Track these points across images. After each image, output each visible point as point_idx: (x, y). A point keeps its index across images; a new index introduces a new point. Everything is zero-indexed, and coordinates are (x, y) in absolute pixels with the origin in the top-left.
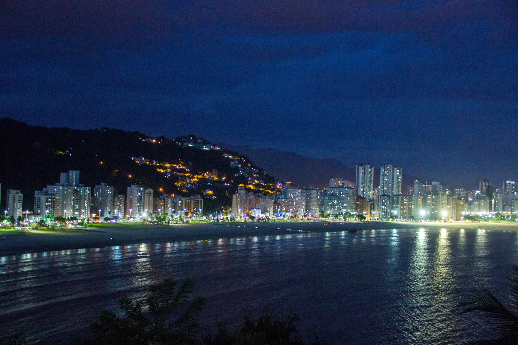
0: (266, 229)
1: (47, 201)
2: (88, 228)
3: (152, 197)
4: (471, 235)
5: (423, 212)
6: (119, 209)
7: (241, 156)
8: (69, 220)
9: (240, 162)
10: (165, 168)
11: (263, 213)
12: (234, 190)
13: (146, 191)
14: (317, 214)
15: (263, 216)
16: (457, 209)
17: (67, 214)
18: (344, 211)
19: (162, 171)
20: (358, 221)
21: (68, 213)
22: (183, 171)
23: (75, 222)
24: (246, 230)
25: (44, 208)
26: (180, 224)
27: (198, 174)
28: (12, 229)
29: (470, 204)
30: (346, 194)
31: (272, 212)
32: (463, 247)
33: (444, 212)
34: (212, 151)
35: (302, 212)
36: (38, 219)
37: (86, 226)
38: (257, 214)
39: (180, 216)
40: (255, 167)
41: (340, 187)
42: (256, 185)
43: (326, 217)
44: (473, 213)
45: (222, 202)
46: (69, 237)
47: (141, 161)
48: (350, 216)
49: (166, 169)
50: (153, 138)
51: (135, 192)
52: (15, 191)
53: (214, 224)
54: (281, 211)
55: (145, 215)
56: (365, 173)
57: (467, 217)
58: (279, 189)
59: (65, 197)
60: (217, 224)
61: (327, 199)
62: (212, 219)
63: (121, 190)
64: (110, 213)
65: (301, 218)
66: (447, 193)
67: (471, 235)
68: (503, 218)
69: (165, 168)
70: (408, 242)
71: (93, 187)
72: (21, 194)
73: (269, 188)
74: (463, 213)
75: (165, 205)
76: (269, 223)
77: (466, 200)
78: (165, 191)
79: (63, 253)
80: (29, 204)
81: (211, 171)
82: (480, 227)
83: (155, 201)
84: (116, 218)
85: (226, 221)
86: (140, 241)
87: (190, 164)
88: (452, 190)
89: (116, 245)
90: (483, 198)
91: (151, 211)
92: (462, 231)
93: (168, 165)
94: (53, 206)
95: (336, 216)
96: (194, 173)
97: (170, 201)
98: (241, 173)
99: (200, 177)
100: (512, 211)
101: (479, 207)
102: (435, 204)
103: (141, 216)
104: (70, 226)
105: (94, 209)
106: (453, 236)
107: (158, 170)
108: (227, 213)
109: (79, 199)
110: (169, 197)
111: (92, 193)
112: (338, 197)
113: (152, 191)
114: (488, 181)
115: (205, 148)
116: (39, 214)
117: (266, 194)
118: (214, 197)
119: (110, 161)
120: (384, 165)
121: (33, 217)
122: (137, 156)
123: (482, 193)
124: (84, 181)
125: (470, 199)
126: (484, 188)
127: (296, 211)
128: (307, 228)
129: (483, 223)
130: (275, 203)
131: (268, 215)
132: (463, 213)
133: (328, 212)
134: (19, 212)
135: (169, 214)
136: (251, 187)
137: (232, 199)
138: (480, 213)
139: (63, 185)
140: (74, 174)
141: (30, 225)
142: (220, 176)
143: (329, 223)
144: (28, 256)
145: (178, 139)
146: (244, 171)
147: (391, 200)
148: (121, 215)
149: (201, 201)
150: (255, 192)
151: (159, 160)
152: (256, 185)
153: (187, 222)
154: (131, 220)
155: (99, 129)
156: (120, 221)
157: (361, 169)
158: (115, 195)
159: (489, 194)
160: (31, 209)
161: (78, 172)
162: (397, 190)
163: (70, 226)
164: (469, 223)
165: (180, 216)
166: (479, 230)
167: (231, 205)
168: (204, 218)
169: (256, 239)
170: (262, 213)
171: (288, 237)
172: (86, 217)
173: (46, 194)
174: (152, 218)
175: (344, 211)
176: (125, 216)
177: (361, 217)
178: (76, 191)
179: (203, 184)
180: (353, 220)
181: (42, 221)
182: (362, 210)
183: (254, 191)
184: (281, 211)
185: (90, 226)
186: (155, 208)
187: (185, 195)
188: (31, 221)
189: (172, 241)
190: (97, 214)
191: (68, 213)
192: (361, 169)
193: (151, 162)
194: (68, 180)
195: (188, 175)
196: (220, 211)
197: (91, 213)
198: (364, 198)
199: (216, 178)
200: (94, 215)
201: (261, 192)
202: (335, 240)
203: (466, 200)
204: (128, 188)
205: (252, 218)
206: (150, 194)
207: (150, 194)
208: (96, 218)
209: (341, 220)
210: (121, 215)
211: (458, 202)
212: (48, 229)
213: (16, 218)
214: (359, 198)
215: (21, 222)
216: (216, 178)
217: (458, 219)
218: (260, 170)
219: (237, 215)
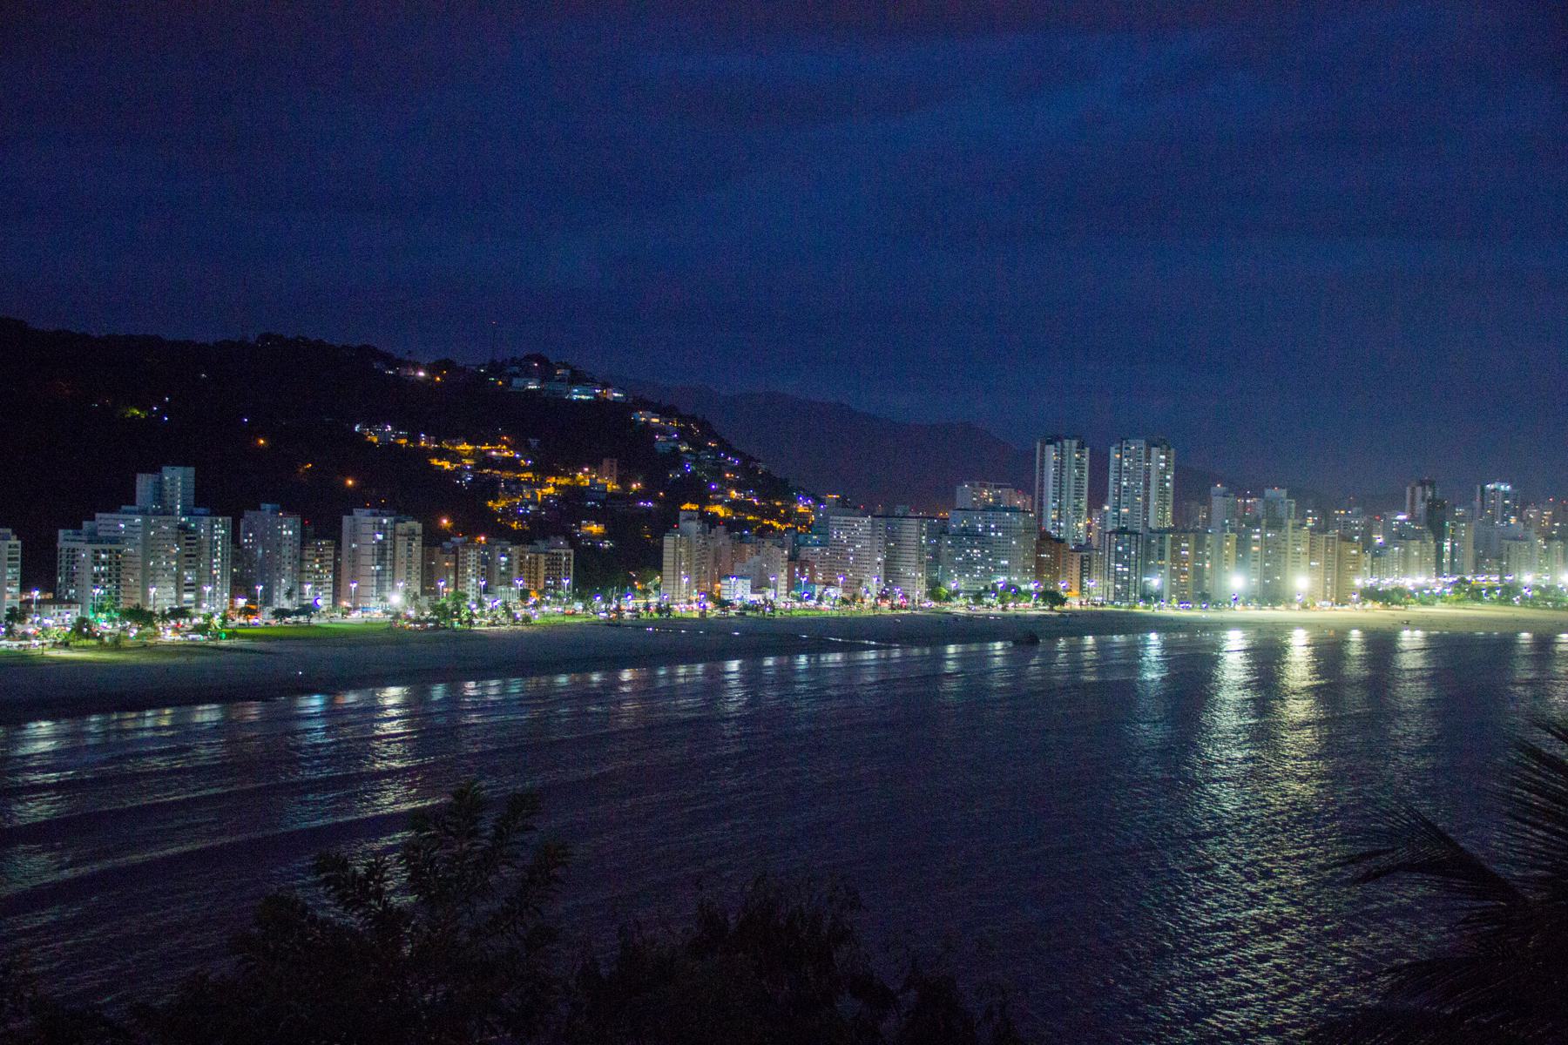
0: (764, 637)
1: (97, 561)
2: (224, 643)
3: (417, 545)
4: (1382, 644)
5: (1237, 581)
6: (319, 583)
7: (681, 418)
8: (164, 617)
9: (684, 435)
10: (455, 457)
11: (755, 589)
12: (667, 521)
13: (399, 526)
14: (919, 591)
16: (1339, 569)
17: (163, 598)
19: (447, 465)
21: (161, 597)
22: (511, 464)
25: (88, 579)
26: (506, 628)
27: (557, 474)
29: (1378, 553)
30: (1007, 530)
31: (782, 587)
32: (1356, 683)
34: (599, 404)
35: (873, 584)
36: (71, 615)
37: (217, 636)
38: (739, 591)
39: (507, 602)
40: (730, 451)
41: (988, 508)
42: (734, 505)
43: (948, 599)
44: (1387, 582)
45: (629, 556)
46: (167, 669)
47: (382, 435)
48: (1018, 594)
49: (459, 458)
50: (417, 367)
51: (367, 529)
53: (609, 624)
56: (1061, 463)
57: (1371, 594)
59: (150, 548)
60: (615, 625)
61: (951, 544)
62: (599, 610)
63: (323, 523)
64: (289, 595)
65: (869, 603)
66: (1310, 523)
67: (1382, 644)
68: (1476, 594)
69: (455, 457)
70: (1193, 668)
72: (14, 541)
73: (773, 513)
74: (1358, 582)
76: (772, 620)
77: (1367, 544)
78: (455, 530)
81: (595, 464)
82: (1408, 624)
83: (427, 558)
84: (306, 610)
85: (645, 615)
87: (534, 442)
89: (310, 692)
90: (1418, 535)
91: (417, 589)
92: (1355, 635)
93: (465, 447)
94: (115, 574)
95: (978, 597)
96: (544, 469)
97: (472, 555)
99: (564, 481)
100: (1503, 572)
101: (1406, 565)
102: (1275, 556)
103: (387, 604)
104: (168, 635)
105: (240, 585)
106: (1329, 652)
107: (435, 462)
109: (193, 553)
113: (418, 526)
114: (1432, 484)
115: (578, 395)
116: (71, 602)
118: (607, 544)
119: (289, 438)
120: (1122, 440)
121: (54, 610)
123: (1413, 519)
124: (207, 499)
125: (1379, 539)
126: (1421, 507)
127: (857, 581)
129: (1416, 611)
130: (793, 558)
131: (770, 594)
132: (1358, 582)
135: (472, 596)
136: (720, 510)
138: (1408, 582)
139: (143, 512)
140: (178, 479)
142: (623, 480)
143: (956, 618)
146: (697, 462)
147: (1142, 545)
149: (566, 553)
152: (734, 505)
153: (527, 619)
154: (356, 616)
155: (252, 340)
157: (1051, 454)
158: (304, 540)
159: (1435, 523)
160: (49, 585)
161: (191, 470)
162: (1160, 516)
163: (168, 636)
164: (1375, 613)
165: (507, 602)
166: (1406, 635)
167: (658, 568)
168: (579, 606)
170: (755, 589)
172: (215, 605)
173: (93, 538)
174: (419, 608)
176: (335, 603)
177: (1054, 598)
178: (184, 528)
179: (574, 503)
180: (1030, 608)
181: (83, 621)
182: (1056, 579)
183: (726, 522)
184: (811, 582)
185: (229, 636)
186: (429, 578)
187: (518, 538)
189: (481, 673)
190: (253, 599)
191: (161, 597)
192: (1051, 454)
193: (414, 438)
194: (159, 494)
196: (626, 586)
197: (233, 596)
198: (1060, 541)
199: (612, 486)
200: (242, 602)
202: (975, 666)
203: (1367, 544)
204: (346, 519)
205: (723, 604)
206: (411, 535)
207: (411, 535)
208: (247, 612)
209: (993, 607)
212: (102, 646)
214: (1046, 540)
215: (17, 627)
216: (612, 486)
217: (1342, 601)
218: (747, 459)
219: (680, 596)
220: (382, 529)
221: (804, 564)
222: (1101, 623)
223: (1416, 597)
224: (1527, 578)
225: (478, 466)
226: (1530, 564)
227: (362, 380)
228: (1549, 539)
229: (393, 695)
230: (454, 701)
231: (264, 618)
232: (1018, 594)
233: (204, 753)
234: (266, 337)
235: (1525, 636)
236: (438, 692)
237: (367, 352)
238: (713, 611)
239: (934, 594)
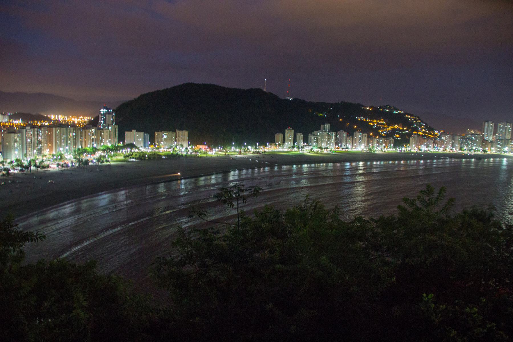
9: (415, 120)
10: (373, 123)
11: (427, 147)
12: (410, 135)
13: (364, 135)
17: (324, 145)
18: (474, 148)
19: (372, 124)
20: (483, 153)
21: (324, 145)
22: (383, 124)
24: (417, 157)
26: (381, 153)
27: (391, 126)
28: (298, 153)
30: (476, 138)
31: (432, 147)
36: (310, 148)
38: (424, 148)
39: (380, 148)
41: (472, 134)
43: (464, 150)
45: (404, 140)
47: (361, 119)
48: (478, 150)
49: (374, 123)
51: (358, 135)
53: (399, 153)
54: (437, 147)
56: (489, 126)
58: (436, 135)
59: (323, 137)
60: (400, 152)
61: (465, 140)
62: (398, 150)
63: (351, 134)
65: (448, 150)
69: (373, 123)
71: (336, 132)
73: (430, 134)
75: (373, 142)
78: (373, 134)
79: (321, 165)
80: (306, 140)
81: (398, 124)
83: (368, 140)
84: (347, 148)
86: (359, 161)
91: (366, 145)
93: (375, 121)
94: (317, 141)
95: (470, 150)
96: (389, 125)
97: (376, 140)
98: (415, 125)
103: (361, 148)
104: (325, 151)
105: (337, 144)
107: (370, 124)
108: (406, 147)
109: (329, 139)
110: (375, 138)
111: (336, 136)
112: (471, 140)
113: (366, 135)
115: (395, 112)
117: (429, 137)
119: (345, 118)
120: (501, 122)
124: (332, 129)
127: (446, 147)
128: (452, 156)
130: (434, 142)
131: (430, 149)
133: (465, 148)
134: (302, 144)
136: (421, 133)
139: (322, 131)
140: (327, 126)
141: (307, 151)
142: (403, 127)
143: (465, 154)
144: (306, 166)
145: (381, 107)
148: (350, 147)
149: (392, 141)
150: (422, 136)
151: (370, 119)
152: (423, 132)
153: (385, 151)
157: (486, 124)
158: (347, 136)
160: (307, 143)
161: (329, 124)
165: (380, 148)
168: (394, 149)
173: (314, 135)
175: (474, 148)
177: (485, 151)
179: (394, 131)
180: (480, 153)
181: (312, 149)
182: (486, 147)
184: (437, 147)
186: (368, 143)
188: (307, 149)
189: (377, 161)
191: (324, 145)
192: (486, 124)
193: (366, 119)
196: (402, 146)
198: (487, 141)
199: (401, 128)
200: (337, 146)
201: (426, 136)
205: (421, 150)
206: (365, 136)
209: (472, 152)
210: (350, 147)
213: (300, 147)
214: (484, 141)
219: (412, 148)
221: (436, 143)
222: (494, 156)
225: (377, 124)
227: (358, 109)
229: (361, 163)
231: (340, 149)
234: (342, 102)
236: (369, 163)
237: (359, 105)
238: (419, 151)
239: (461, 149)
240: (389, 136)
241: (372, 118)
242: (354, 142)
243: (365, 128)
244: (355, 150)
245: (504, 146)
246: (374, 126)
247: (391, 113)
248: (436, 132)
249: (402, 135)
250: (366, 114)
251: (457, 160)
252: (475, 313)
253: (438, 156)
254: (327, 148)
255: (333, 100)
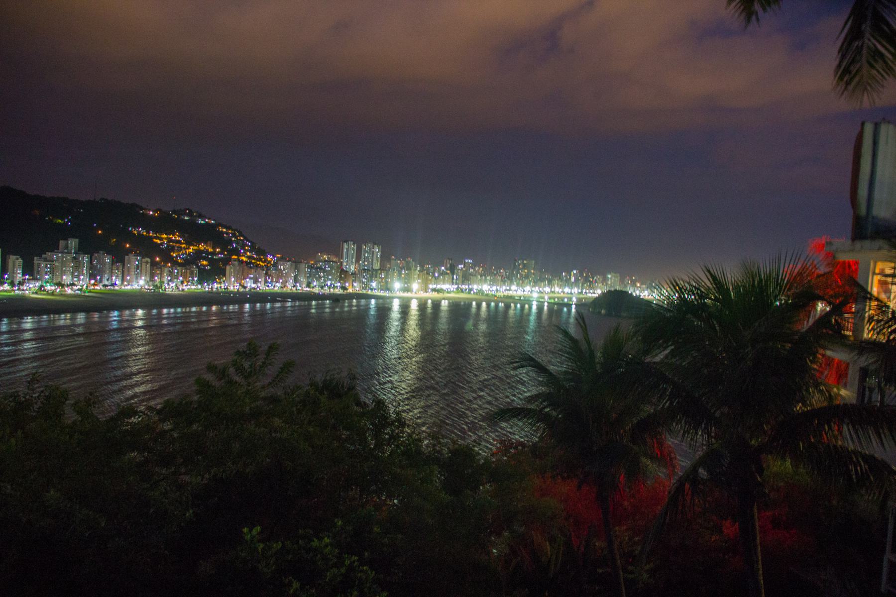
1: (46, 267)
4: (436, 305)
5: (397, 285)
6: (117, 277)
8: (68, 286)
9: (234, 235)
10: (161, 239)
11: (256, 282)
12: (227, 261)
15: (254, 286)
17: (66, 279)
19: (159, 241)
20: (341, 292)
21: (67, 279)
22: (179, 242)
23: (75, 288)
24: (240, 298)
25: (44, 273)
26: (177, 292)
27: (193, 245)
28: (12, 293)
29: (436, 278)
31: (263, 283)
32: (429, 315)
33: (415, 286)
35: (291, 282)
38: (250, 284)
40: (247, 240)
41: (325, 261)
42: (249, 257)
44: (439, 287)
45: (217, 271)
47: (139, 232)
48: (334, 287)
50: (150, 210)
51: (134, 261)
52: (15, 257)
53: (209, 292)
55: (142, 282)
56: (349, 248)
57: (434, 290)
58: (270, 262)
59: (63, 264)
61: (315, 271)
62: (207, 288)
63: (119, 258)
65: (290, 287)
67: (436, 305)
68: (462, 291)
69: (161, 239)
70: (384, 311)
72: (20, 260)
73: (260, 260)
74: (431, 286)
76: (257, 293)
77: (434, 275)
78: (161, 261)
80: (30, 270)
81: (206, 243)
82: (444, 299)
83: (152, 269)
86: (137, 308)
87: (186, 235)
88: (422, 266)
89: (114, 310)
92: (430, 301)
93: (165, 236)
94: (52, 272)
95: (322, 287)
96: (189, 244)
97: (166, 270)
99: (195, 248)
102: (408, 279)
103: (139, 284)
104: (69, 291)
105: (92, 276)
106: (422, 307)
108: (220, 283)
109: (78, 267)
110: (165, 266)
111: (91, 261)
112: (324, 270)
113: (149, 260)
117: (257, 266)
119: (107, 230)
120: (366, 243)
121: (32, 282)
122: (134, 227)
123: (446, 269)
124: (83, 249)
127: (288, 282)
128: (295, 297)
130: (266, 274)
132: (431, 286)
134: (19, 277)
136: (244, 259)
137: (225, 270)
138: (445, 287)
139: (62, 253)
140: (73, 243)
141: (30, 289)
143: (315, 294)
145: (174, 212)
146: (238, 244)
147: (372, 274)
149: (196, 271)
152: (249, 257)
154: (129, 287)
155: (97, 200)
156: (116, 288)
157: (346, 246)
158: (113, 263)
160: (31, 274)
161: (77, 240)
162: (377, 265)
163: (69, 291)
164: (435, 295)
167: (224, 275)
168: (199, 287)
169: (247, 306)
170: (254, 283)
171: (278, 305)
173: (46, 260)
175: (329, 283)
176: (122, 283)
177: (344, 288)
179: (198, 255)
180: (338, 291)
181: (42, 286)
182: (345, 282)
183: (246, 262)
186: (152, 276)
187: (180, 265)
188: (31, 286)
191: (67, 279)
193: (148, 232)
194: (67, 247)
195: (183, 246)
196: (214, 281)
197: (90, 280)
199: (210, 250)
200: (93, 282)
201: (253, 263)
202: (320, 307)
205: (245, 287)
206: (147, 262)
208: (94, 285)
209: (326, 290)
211: (427, 276)
212: (48, 294)
213: (17, 283)
215: (22, 288)
216: (210, 250)
217: (426, 292)
220: (137, 260)
222: (359, 296)
223: (446, 291)
224: (475, 287)
226: (476, 283)
227: (132, 213)
228: (481, 276)
229: (140, 312)
230: (160, 314)
232: (334, 287)
233: (80, 330)
234: (102, 199)
235: (474, 303)
236: (155, 311)
237: (134, 206)
238: (242, 290)
239: (308, 285)
240: (189, 262)
241: (159, 230)
242: (126, 273)
243: (146, 248)
244: (129, 287)
245: (370, 280)
246: (162, 244)
247: (192, 224)
248: (270, 258)
249: (212, 262)
250: (148, 223)
251: (303, 303)
252: (326, 546)
253: (273, 297)
254: (73, 284)
255: (83, 199)
